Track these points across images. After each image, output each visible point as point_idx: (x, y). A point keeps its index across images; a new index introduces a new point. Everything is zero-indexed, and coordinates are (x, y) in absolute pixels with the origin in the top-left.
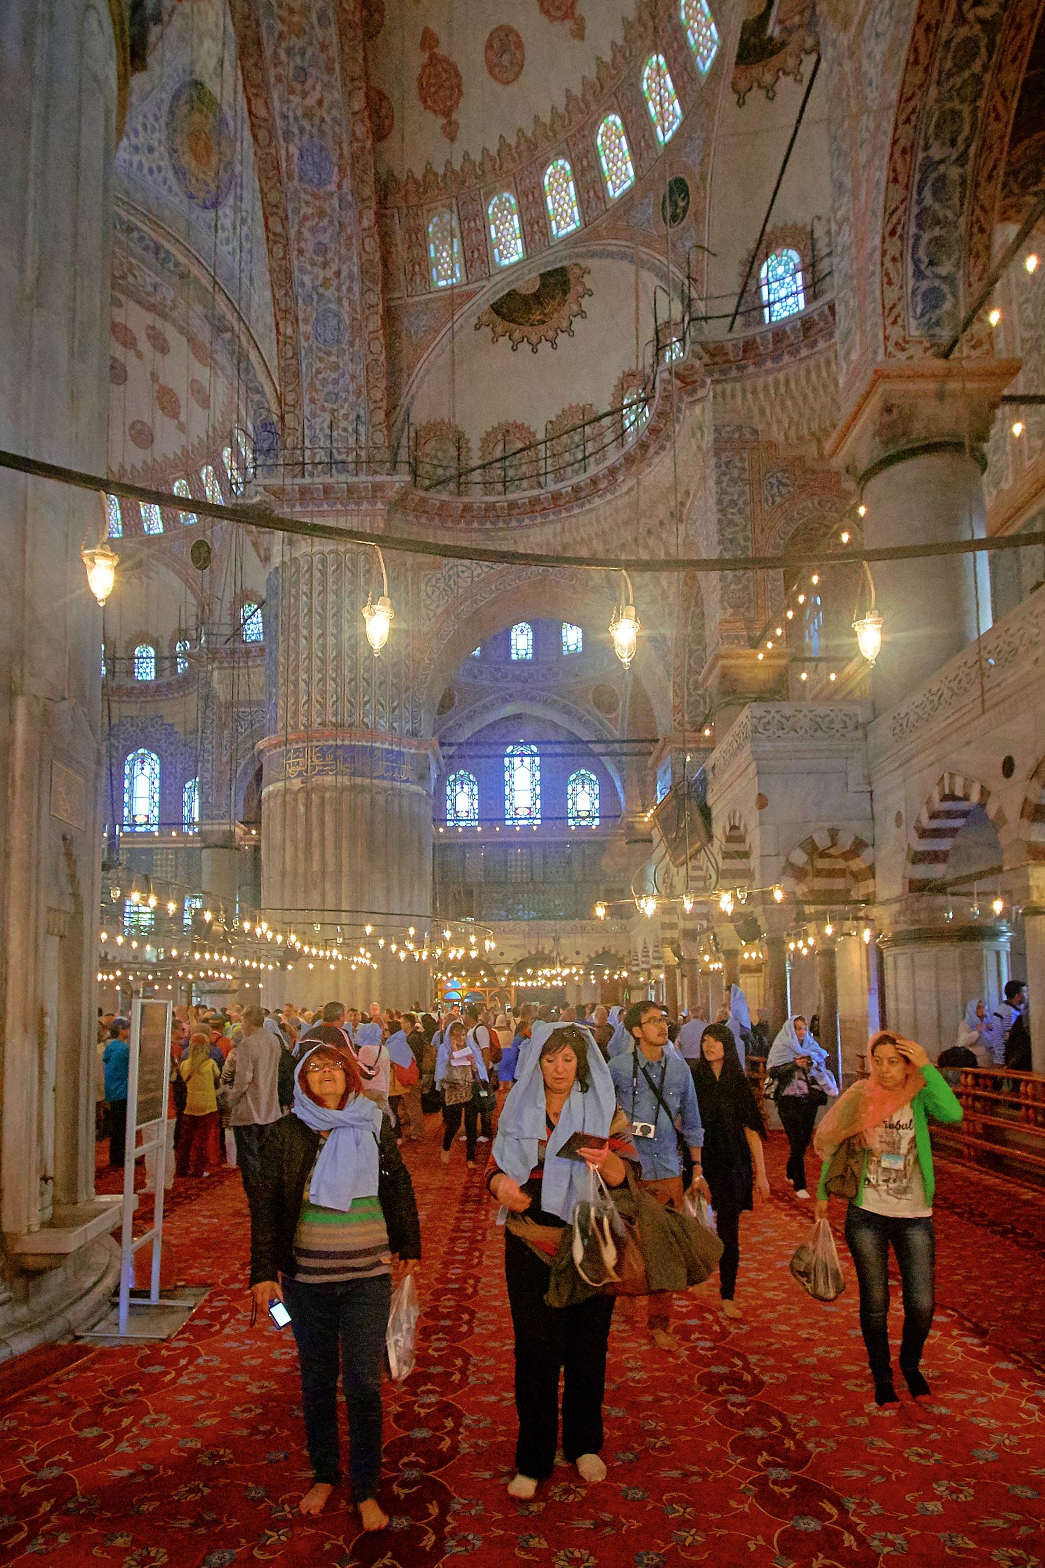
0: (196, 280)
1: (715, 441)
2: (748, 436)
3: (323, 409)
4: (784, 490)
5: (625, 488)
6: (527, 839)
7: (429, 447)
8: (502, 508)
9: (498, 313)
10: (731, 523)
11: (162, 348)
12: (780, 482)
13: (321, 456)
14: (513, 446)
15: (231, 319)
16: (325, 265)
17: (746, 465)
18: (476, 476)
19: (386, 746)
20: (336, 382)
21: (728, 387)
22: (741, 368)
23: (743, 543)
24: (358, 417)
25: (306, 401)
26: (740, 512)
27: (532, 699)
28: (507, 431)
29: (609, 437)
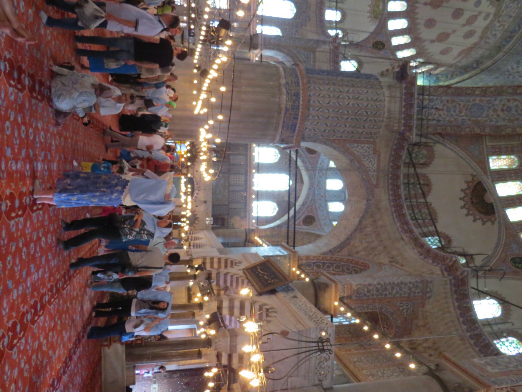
1: (427, 281)
2: (428, 295)
3: (444, 106)
4: (405, 311)
6: (247, 183)
7: (424, 152)
9: (477, 184)
10: (393, 289)
12: (408, 309)
13: (426, 103)
14: (424, 187)
15: (482, 67)
16: (502, 110)
17: (416, 294)
18: (412, 170)
19: (298, 125)
20: (455, 111)
21: (448, 287)
22: (456, 292)
23: (384, 293)
24: (439, 121)
26: (397, 292)
27: (310, 189)
28: (428, 185)
29: (425, 230)
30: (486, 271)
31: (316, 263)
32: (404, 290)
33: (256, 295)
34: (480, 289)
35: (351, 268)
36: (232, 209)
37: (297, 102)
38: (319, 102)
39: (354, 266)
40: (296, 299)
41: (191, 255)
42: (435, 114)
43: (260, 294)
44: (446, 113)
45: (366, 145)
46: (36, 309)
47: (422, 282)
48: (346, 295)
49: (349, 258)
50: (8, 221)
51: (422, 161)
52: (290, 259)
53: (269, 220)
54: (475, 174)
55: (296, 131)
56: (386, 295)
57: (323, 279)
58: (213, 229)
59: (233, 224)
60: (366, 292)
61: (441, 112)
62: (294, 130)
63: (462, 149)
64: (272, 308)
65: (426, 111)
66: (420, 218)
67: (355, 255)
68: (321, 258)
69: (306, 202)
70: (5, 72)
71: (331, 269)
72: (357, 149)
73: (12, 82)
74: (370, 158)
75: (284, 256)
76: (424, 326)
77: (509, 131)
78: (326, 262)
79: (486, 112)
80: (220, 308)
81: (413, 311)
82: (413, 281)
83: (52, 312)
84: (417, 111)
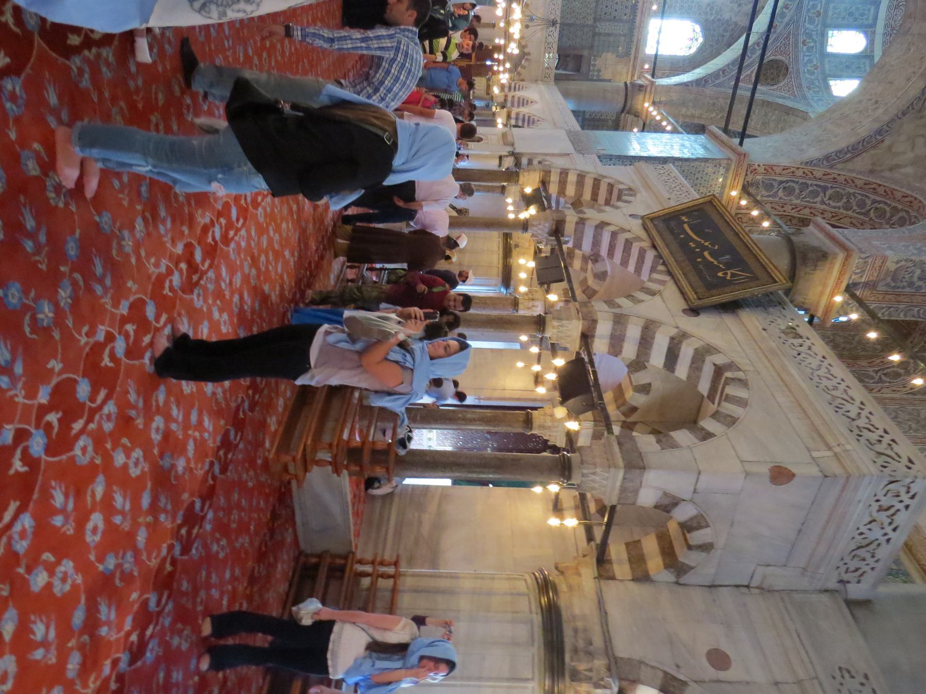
31: (787, 182)
33: (684, 311)
35: (869, 202)
36: (600, 34)
39: (878, 199)
40: (797, 341)
41: (513, 145)
43: (694, 311)
46: (229, 218)
48: (863, 280)
49: (871, 179)
52: (727, 170)
53: (679, 65)
57: (813, 236)
58: (558, 79)
59: (599, 71)
60: (915, 279)
64: (731, 366)
67: (887, 174)
68: (800, 173)
71: (819, 199)
75: (716, 162)
78: (809, 182)
80: (586, 338)
83: (261, 220)
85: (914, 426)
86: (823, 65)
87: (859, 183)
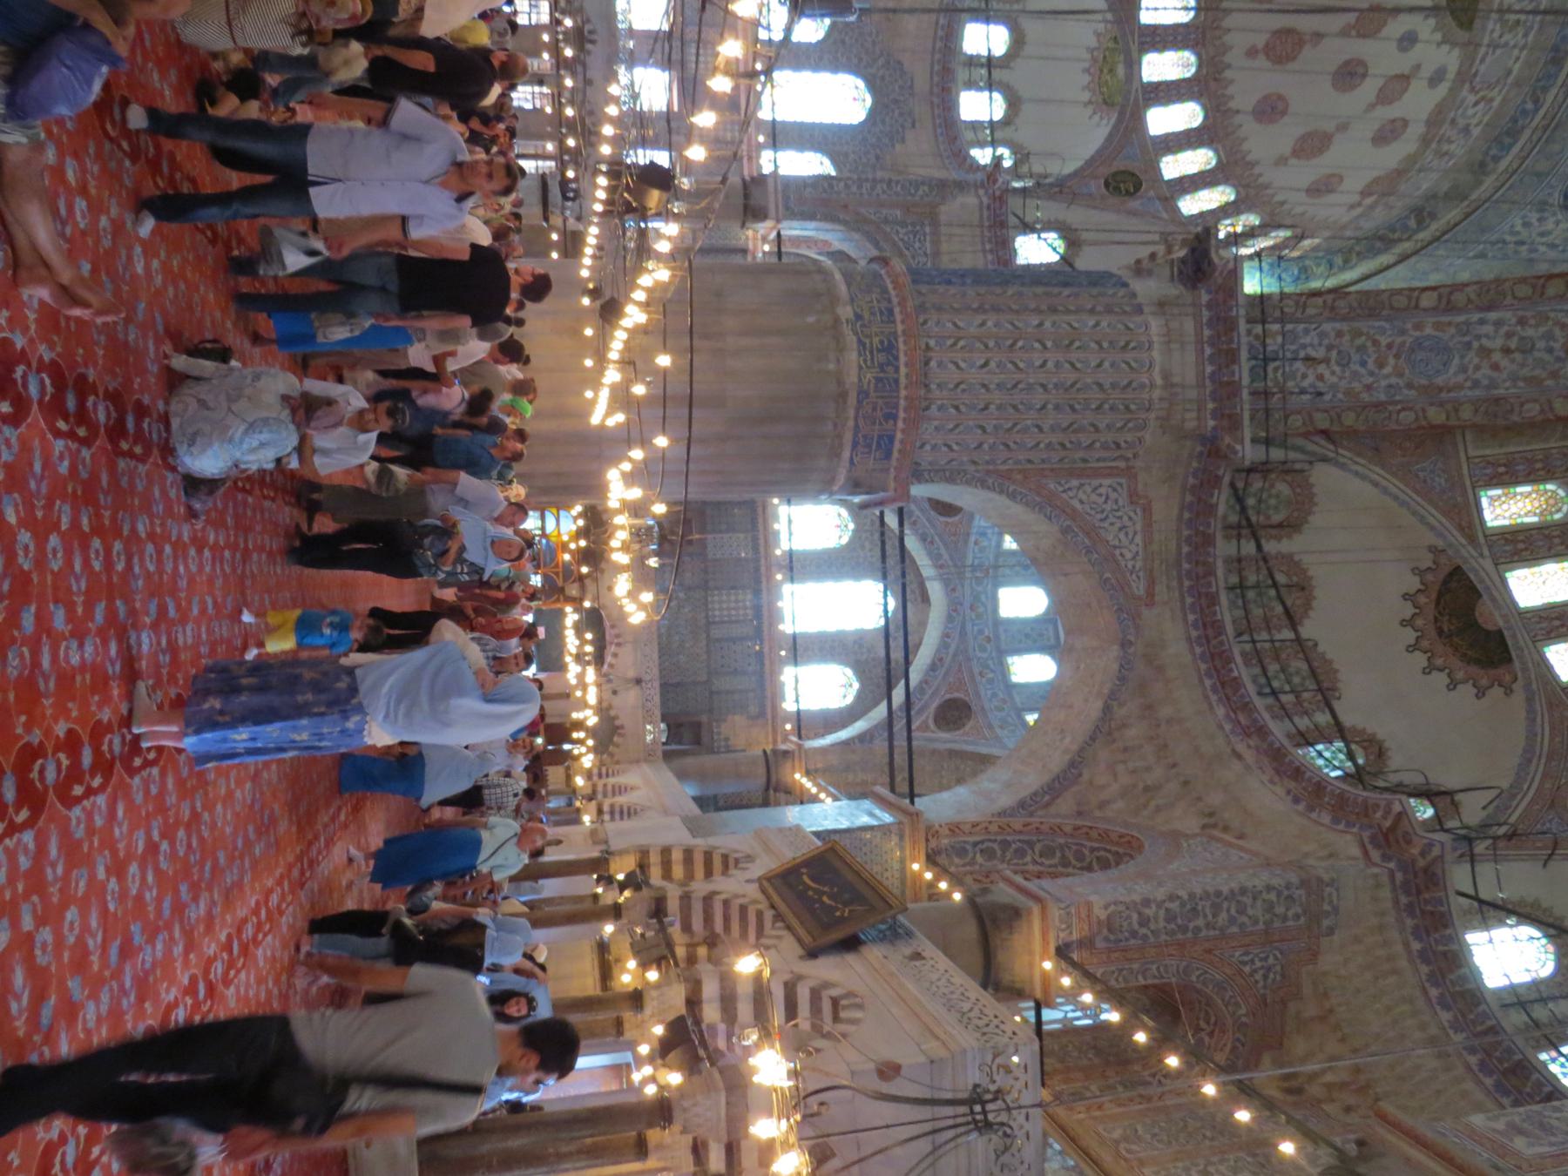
0: (1479, 183)
1: (1320, 880)
2: (1326, 923)
3: (1330, 348)
4: (1258, 976)
5: (1241, 748)
6: (763, 616)
7: (1283, 488)
8: (1209, 584)
9: (1451, 575)
10: (1216, 908)
11: (1387, 134)
12: (1269, 969)
13: (1273, 344)
14: (1291, 594)
15: (1435, 227)
16: (1507, 351)
17: (1290, 923)
18: (1249, 548)
19: (899, 435)
20: (1363, 364)
21: (1386, 893)
22: (1410, 909)
23: (1191, 925)
24: (1320, 394)
25: (1338, 325)
26: (1232, 920)
27: (950, 618)
28: (1303, 587)
29: (1303, 723)
30: (1496, 838)
31: (982, 842)
32: (1250, 912)
33: (801, 957)
34: (1483, 895)
35: (1087, 852)
36: (718, 693)
37: (890, 369)
38: (956, 364)
39: (1096, 845)
40: (917, 963)
41: (606, 842)
42: (1304, 376)
43: (812, 954)
44: (1337, 369)
45: (1107, 482)
47: (1304, 883)
48: (1075, 937)
49: (1079, 822)
50: (64, 811)
51: (1277, 518)
52: (901, 837)
54: (1440, 544)
55: (895, 454)
56: (1197, 929)
57: (1003, 893)
58: (668, 756)
59: (727, 739)
60: (1136, 926)
61: (1322, 369)
62: (888, 455)
63: (1394, 474)
64: (850, 994)
65: (1276, 369)
66: (1287, 688)
67: (1098, 813)
68: (994, 828)
69: (941, 659)
70: (40, 402)
71: (1028, 859)
72: (1081, 495)
73: (62, 425)
74: (1120, 518)
75: (883, 829)
76: (1322, 1019)
77: (1532, 410)
79: (1456, 361)
80: (693, 1002)
81: (1283, 976)
82: (1275, 882)
84: (1252, 369)
85: (1208, 1134)
86: (1012, 698)
87: (1068, 829)
